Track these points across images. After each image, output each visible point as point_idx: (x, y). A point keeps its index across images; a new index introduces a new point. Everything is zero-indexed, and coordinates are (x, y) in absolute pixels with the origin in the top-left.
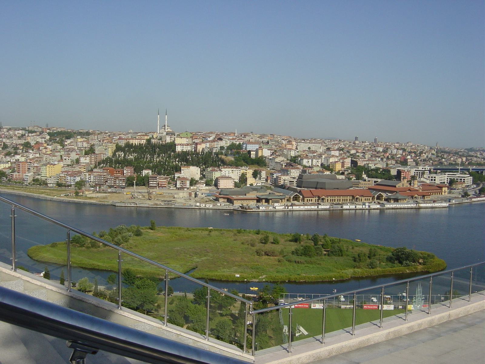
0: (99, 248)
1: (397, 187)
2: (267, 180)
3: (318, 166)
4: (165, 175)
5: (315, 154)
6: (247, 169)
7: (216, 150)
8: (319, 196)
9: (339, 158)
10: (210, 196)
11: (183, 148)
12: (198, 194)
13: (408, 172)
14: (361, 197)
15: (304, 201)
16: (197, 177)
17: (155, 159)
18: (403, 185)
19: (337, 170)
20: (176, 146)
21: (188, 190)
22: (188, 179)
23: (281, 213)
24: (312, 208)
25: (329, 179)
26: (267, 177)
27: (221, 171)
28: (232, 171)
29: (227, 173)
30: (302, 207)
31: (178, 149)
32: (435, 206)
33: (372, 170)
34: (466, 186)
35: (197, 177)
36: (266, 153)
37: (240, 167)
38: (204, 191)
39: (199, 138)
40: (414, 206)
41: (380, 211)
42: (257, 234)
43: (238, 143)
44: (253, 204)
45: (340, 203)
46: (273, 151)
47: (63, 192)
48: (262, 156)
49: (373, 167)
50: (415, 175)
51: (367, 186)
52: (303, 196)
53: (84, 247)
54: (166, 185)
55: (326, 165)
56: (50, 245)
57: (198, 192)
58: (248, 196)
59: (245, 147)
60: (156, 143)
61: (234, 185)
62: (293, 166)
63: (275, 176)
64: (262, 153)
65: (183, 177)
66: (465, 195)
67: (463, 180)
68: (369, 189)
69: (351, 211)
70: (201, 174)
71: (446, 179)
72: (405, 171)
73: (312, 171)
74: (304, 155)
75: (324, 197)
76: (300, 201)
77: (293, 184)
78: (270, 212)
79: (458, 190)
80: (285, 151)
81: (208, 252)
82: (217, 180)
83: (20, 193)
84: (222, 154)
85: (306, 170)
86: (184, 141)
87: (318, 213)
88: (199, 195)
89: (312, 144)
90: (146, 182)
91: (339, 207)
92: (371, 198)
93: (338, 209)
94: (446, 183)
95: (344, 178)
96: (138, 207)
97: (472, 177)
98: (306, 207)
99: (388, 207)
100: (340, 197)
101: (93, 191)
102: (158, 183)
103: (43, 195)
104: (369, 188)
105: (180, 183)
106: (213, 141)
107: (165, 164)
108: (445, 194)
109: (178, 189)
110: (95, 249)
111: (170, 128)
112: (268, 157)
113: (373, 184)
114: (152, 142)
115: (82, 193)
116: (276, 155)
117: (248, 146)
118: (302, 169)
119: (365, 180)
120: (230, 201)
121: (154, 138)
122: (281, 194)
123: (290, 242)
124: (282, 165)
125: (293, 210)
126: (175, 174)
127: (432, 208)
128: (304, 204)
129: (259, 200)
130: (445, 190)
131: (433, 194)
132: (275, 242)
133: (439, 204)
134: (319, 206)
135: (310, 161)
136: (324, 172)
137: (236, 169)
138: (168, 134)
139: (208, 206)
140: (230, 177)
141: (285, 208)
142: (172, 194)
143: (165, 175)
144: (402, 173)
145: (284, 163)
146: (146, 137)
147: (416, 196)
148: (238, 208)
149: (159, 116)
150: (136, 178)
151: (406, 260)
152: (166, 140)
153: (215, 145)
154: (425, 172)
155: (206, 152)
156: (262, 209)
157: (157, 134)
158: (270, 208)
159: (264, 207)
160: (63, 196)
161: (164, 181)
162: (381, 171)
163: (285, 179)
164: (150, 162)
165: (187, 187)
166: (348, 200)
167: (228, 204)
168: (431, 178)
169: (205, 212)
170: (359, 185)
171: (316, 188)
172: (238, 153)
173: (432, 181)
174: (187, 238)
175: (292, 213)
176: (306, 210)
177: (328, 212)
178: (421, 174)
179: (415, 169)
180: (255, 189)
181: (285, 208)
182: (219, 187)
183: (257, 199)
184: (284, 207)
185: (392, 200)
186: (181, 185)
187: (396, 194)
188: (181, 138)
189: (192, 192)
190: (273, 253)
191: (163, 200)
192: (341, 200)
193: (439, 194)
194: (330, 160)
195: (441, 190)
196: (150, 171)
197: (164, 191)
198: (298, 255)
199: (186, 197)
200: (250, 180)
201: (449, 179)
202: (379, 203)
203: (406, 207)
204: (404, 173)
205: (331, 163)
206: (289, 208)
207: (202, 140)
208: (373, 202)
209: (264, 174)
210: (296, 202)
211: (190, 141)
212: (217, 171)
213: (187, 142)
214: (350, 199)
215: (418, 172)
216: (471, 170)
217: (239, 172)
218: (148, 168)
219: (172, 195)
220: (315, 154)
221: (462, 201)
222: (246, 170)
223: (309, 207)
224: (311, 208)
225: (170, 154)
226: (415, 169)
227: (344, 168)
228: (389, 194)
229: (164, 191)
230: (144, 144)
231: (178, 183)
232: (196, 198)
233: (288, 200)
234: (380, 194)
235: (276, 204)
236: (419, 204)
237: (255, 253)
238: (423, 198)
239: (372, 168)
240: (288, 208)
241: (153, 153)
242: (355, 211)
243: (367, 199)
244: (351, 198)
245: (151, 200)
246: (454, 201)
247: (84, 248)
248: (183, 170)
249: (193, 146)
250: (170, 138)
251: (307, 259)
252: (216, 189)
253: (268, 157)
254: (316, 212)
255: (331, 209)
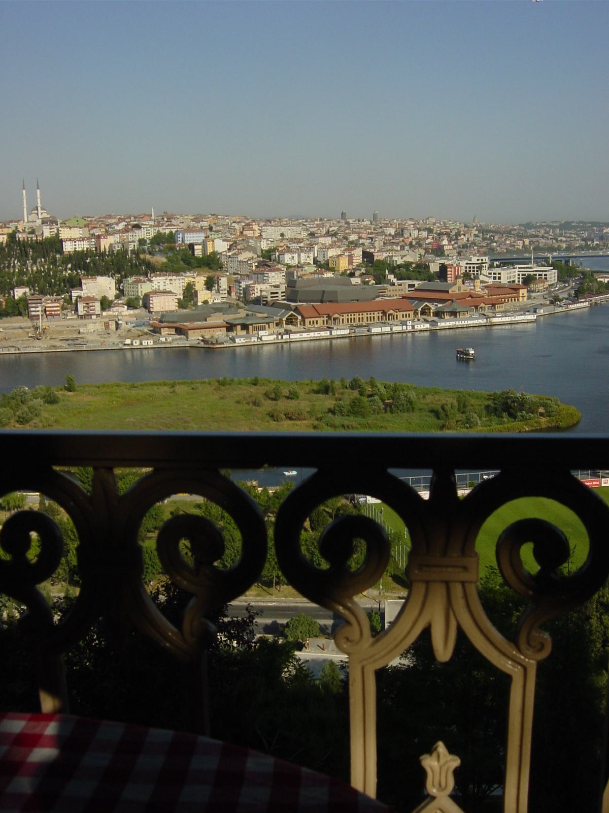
1: (450, 292)
2: (229, 293)
3: (309, 264)
4: (53, 295)
5: (302, 245)
6: (195, 275)
7: (134, 246)
8: (328, 315)
9: (343, 249)
10: (141, 326)
11: (75, 245)
12: (121, 324)
13: (458, 268)
14: (397, 312)
15: (304, 324)
16: (111, 294)
17: (29, 269)
18: (459, 288)
19: (342, 270)
20: (64, 243)
21: (98, 318)
22: (96, 300)
23: (272, 347)
24: (321, 336)
25: (339, 285)
26: (230, 287)
27: (151, 281)
28: (171, 280)
29: (162, 284)
30: (305, 335)
31: (66, 247)
32: (516, 321)
33: (399, 266)
34: (549, 285)
35: (111, 294)
36: (220, 246)
37: (182, 273)
38: (126, 317)
39: (100, 227)
40: (483, 322)
41: (430, 333)
42: (255, 384)
43: (167, 231)
44: (220, 334)
45: (364, 324)
46: (231, 243)
48: (214, 251)
49: (400, 261)
50: (466, 271)
51: (398, 293)
52: (303, 317)
54: (59, 312)
55: (322, 262)
57: (121, 320)
58: (211, 321)
59: (182, 238)
60: (26, 239)
61: (177, 304)
62: (270, 267)
63: (243, 285)
64: (213, 247)
65: (85, 296)
66: (555, 300)
67: (543, 275)
68: (403, 298)
69: (384, 336)
70: (116, 289)
71: (517, 275)
72: (453, 265)
73: (303, 273)
74: (282, 247)
75: (336, 316)
76: (299, 325)
77: (277, 297)
78: (253, 347)
79: (538, 292)
80: (251, 241)
81: (185, 422)
82: (147, 297)
84: (144, 252)
85: (294, 273)
86: (76, 233)
87: (331, 343)
88: (123, 325)
89: (287, 228)
90: (22, 310)
91: (363, 331)
92: (412, 313)
93: (364, 334)
94: (516, 282)
95: (360, 282)
96: (22, 353)
97: (556, 271)
98: (312, 334)
99: (442, 327)
100: (354, 315)
102: (45, 309)
104: (403, 297)
105: (84, 307)
106: (126, 230)
107: (49, 275)
108: (523, 300)
109: (81, 317)
111: (45, 212)
112: (225, 253)
113: (407, 289)
114: (19, 238)
116: (238, 249)
117: (186, 235)
118: (285, 270)
119: (393, 284)
120: (180, 331)
121: (19, 231)
122: (266, 315)
123: (316, 395)
124: (251, 265)
125: (291, 340)
126: (73, 292)
127: (511, 324)
128: (305, 328)
129: (230, 327)
130: (523, 294)
131: (508, 300)
132: (292, 396)
133: (522, 317)
134: (333, 332)
135: (296, 256)
136: (324, 274)
137: (177, 276)
138: (44, 222)
139: (146, 344)
140: (170, 292)
141: (277, 339)
142: (73, 326)
143: (53, 295)
144: (449, 270)
145: (254, 263)
146: (6, 231)
147: (482, 305)
148: (199, 343)
149: (24, 191)
150: (4, 304)
151: (521, 411)
152: (43, 233)
153: (130, 237)
154: (484, 265)
155: (118, 250)
156: (240, 342)
157: (25, 224)
158: (252, 340)
159: (242, 339)
161: (56, 305)
162: (414, 268)
163: (259, 289)
164: (21, 273)
165: (96, 313)
166: (376, 319)
167: (178, 337)
168: (493, 275)
169: (142, 354)
170: (385, 292)
171: (322, 302)
172: (172, 249)
173: (496, 279)
174: (138, 400)
175: (290, 345)
176: (311, 339)
177: (347, 340)
178: (476, 269)
179: (466, 262)
180: (217, 309)
181: (277, 339)
182: (151, 310)
183: (227, 325)
184: (275, 336)
185: (445, 314)
186: (86, 311)
187: (451, 304)
188: (70, 228)
189: (110, 322)
190: (299, 414)
191: (61, 339)
192: (365, 320)
193: (515, 300)
194: (329, 253)
195: (517, 293)
196: (27, 290)
197: (58, 323)
198: (343, 415)
199: (100, 330)
200: (203, 295)
201: (521, 275)
202: (426, 321)
203: (470, 324)
204: (451, 268)
205: (330, 257)
206: (285, 337)
207: (106, 229)
208: (416, 320)
209: (224, 283)
210: (290, 327)
211: (85, 233)
212: (144, 282)
213: (81, 234)
214: (379, 317)
215: (472, 266)
216: (551, 259)
217: (181, 281)
218: (20, 284)
219: (74, 328)
220: (302, 245)
221: (554, 310)
222: (194, 278)
223: (316, 333)
224: (319, 335)
225: (55, 258)
226: (466, 262)
227: (352, 265)
228: (440, 305)
229: (58, 323)
230: (5, 242)
231: (81, 306)
232: (118, 330)
233: (277, 325)
234: (426, 305)
235: (261, 333)
236: (491, 319)
237: (268, 418)
238: (493, 307)
239: (398, 263)
240: (282, 338)
241: (23, 256)
242: (392, 336)
243: (406, 315)
244: (380, 315)
245: (39, 339)
246: (542, 311)
248: (85, 284)
249: (92, 242)
250: (51, 229)
251: (360, 419)
252: (148, 313)
253: (225, 253)
254: (328, 342)
255: (353, 335)
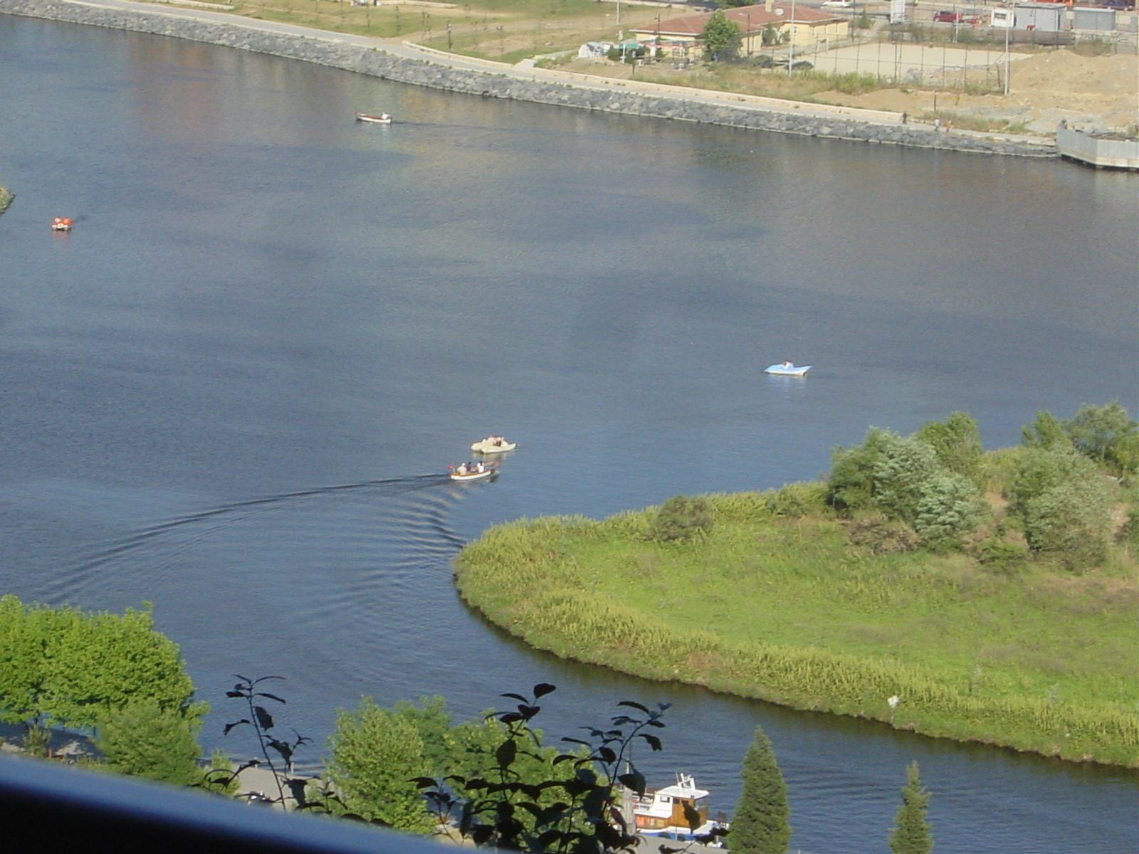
0: (1096, 571)
47: (595, 25)
53: (958, 548)
56: (643, 518)
83: (196, 25)
101: (852, 26)
103: (407, 48)
110: (1074, 579)
115: (758, 40)
160: (595, 57)
247: (958, 561)
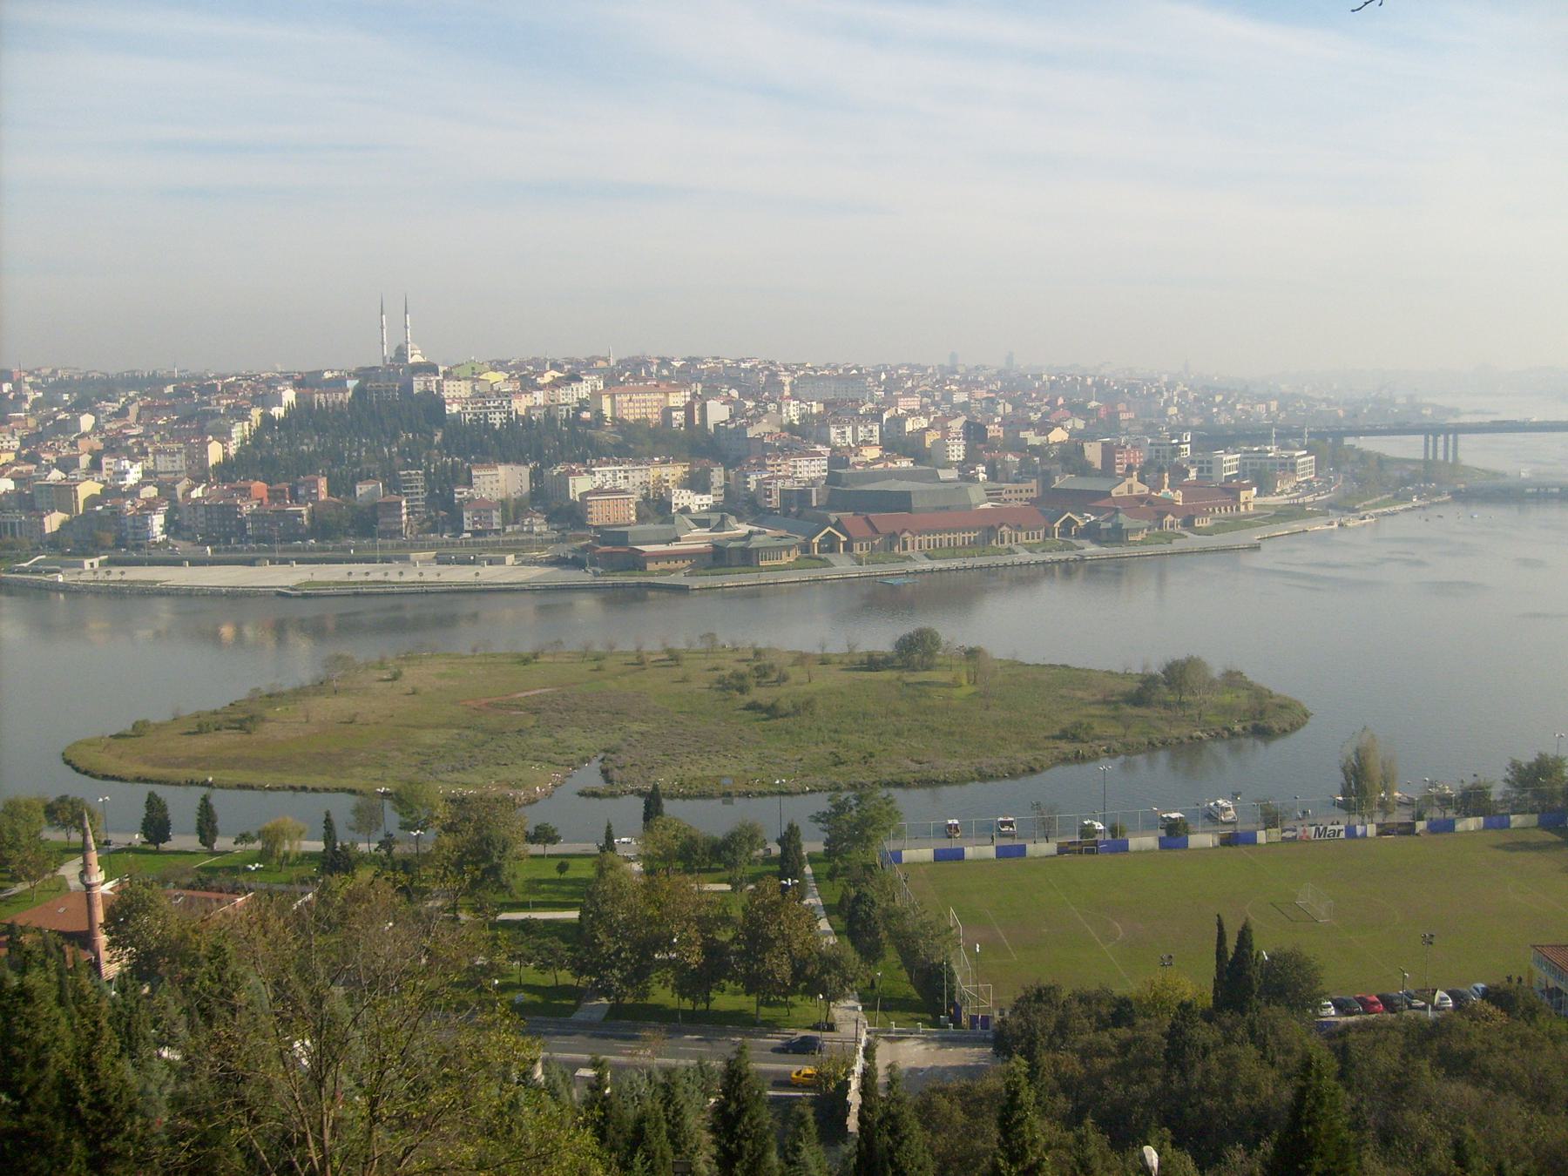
1: (1114, 495)
7: (568, 411)
18: (1130, 487)
131: (1214, 510)
135: (849, 430)
170: (1001, 494)
212: (580, 474)
